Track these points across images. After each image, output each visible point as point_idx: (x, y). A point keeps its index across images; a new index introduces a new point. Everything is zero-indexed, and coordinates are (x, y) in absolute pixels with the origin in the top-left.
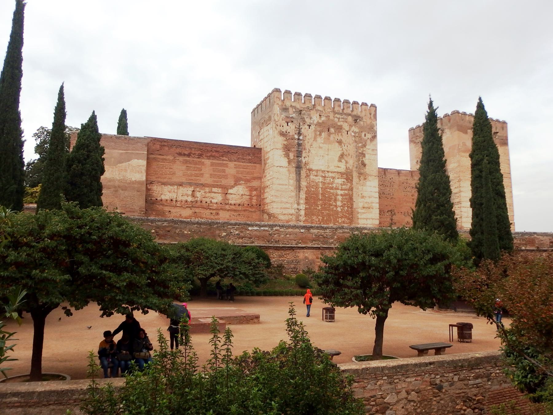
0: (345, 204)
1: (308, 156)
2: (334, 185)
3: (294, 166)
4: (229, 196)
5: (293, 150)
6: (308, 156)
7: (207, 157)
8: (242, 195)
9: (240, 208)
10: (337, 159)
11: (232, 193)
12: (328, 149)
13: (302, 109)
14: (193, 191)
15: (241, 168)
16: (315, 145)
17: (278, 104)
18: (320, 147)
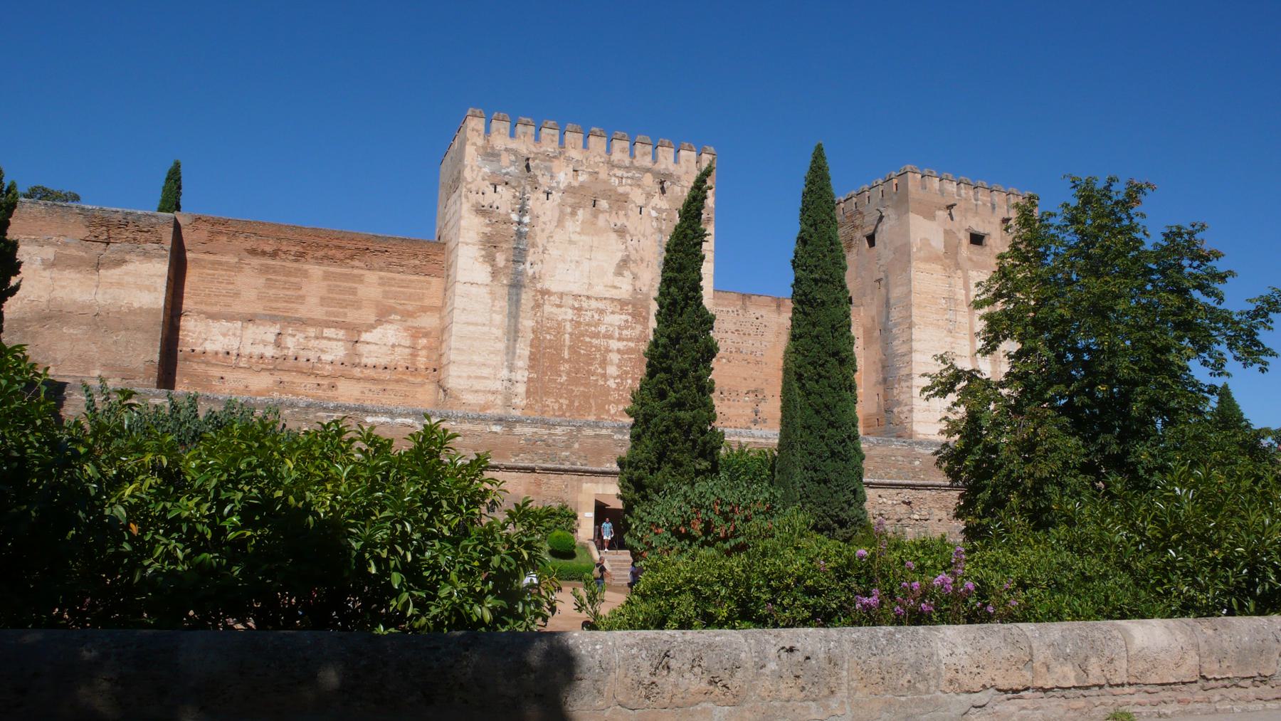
0: (627, 373)
1: (542, 261)
2: (602, 329)
3: (505, 282)
4: (361, 348)
5: (505, 246)
6: (542, 261)
7: (317, 258)
8: (393, 346)
9: (387, 375)
10: (611, 269)
11: (369, 340)
12: (592, 247)
13: (532, 156)
14: (279, 334)
15: (393, 286)
16: (559, 236)
17: (474, 144)
18: (571, 242)
